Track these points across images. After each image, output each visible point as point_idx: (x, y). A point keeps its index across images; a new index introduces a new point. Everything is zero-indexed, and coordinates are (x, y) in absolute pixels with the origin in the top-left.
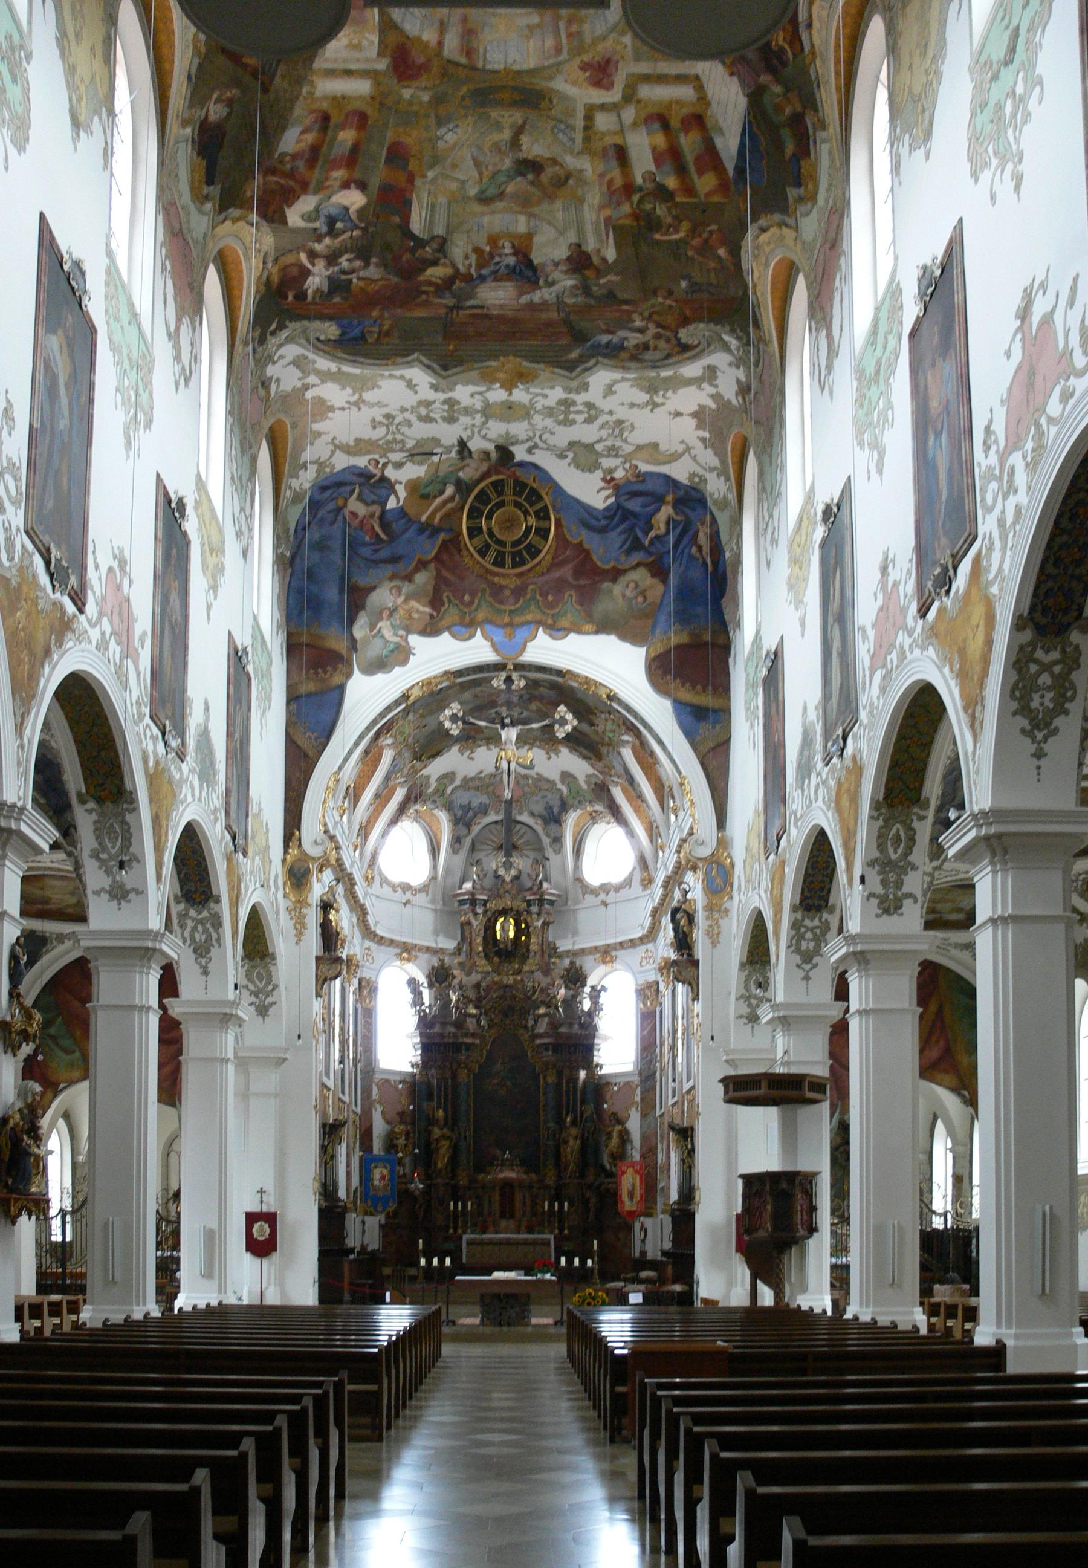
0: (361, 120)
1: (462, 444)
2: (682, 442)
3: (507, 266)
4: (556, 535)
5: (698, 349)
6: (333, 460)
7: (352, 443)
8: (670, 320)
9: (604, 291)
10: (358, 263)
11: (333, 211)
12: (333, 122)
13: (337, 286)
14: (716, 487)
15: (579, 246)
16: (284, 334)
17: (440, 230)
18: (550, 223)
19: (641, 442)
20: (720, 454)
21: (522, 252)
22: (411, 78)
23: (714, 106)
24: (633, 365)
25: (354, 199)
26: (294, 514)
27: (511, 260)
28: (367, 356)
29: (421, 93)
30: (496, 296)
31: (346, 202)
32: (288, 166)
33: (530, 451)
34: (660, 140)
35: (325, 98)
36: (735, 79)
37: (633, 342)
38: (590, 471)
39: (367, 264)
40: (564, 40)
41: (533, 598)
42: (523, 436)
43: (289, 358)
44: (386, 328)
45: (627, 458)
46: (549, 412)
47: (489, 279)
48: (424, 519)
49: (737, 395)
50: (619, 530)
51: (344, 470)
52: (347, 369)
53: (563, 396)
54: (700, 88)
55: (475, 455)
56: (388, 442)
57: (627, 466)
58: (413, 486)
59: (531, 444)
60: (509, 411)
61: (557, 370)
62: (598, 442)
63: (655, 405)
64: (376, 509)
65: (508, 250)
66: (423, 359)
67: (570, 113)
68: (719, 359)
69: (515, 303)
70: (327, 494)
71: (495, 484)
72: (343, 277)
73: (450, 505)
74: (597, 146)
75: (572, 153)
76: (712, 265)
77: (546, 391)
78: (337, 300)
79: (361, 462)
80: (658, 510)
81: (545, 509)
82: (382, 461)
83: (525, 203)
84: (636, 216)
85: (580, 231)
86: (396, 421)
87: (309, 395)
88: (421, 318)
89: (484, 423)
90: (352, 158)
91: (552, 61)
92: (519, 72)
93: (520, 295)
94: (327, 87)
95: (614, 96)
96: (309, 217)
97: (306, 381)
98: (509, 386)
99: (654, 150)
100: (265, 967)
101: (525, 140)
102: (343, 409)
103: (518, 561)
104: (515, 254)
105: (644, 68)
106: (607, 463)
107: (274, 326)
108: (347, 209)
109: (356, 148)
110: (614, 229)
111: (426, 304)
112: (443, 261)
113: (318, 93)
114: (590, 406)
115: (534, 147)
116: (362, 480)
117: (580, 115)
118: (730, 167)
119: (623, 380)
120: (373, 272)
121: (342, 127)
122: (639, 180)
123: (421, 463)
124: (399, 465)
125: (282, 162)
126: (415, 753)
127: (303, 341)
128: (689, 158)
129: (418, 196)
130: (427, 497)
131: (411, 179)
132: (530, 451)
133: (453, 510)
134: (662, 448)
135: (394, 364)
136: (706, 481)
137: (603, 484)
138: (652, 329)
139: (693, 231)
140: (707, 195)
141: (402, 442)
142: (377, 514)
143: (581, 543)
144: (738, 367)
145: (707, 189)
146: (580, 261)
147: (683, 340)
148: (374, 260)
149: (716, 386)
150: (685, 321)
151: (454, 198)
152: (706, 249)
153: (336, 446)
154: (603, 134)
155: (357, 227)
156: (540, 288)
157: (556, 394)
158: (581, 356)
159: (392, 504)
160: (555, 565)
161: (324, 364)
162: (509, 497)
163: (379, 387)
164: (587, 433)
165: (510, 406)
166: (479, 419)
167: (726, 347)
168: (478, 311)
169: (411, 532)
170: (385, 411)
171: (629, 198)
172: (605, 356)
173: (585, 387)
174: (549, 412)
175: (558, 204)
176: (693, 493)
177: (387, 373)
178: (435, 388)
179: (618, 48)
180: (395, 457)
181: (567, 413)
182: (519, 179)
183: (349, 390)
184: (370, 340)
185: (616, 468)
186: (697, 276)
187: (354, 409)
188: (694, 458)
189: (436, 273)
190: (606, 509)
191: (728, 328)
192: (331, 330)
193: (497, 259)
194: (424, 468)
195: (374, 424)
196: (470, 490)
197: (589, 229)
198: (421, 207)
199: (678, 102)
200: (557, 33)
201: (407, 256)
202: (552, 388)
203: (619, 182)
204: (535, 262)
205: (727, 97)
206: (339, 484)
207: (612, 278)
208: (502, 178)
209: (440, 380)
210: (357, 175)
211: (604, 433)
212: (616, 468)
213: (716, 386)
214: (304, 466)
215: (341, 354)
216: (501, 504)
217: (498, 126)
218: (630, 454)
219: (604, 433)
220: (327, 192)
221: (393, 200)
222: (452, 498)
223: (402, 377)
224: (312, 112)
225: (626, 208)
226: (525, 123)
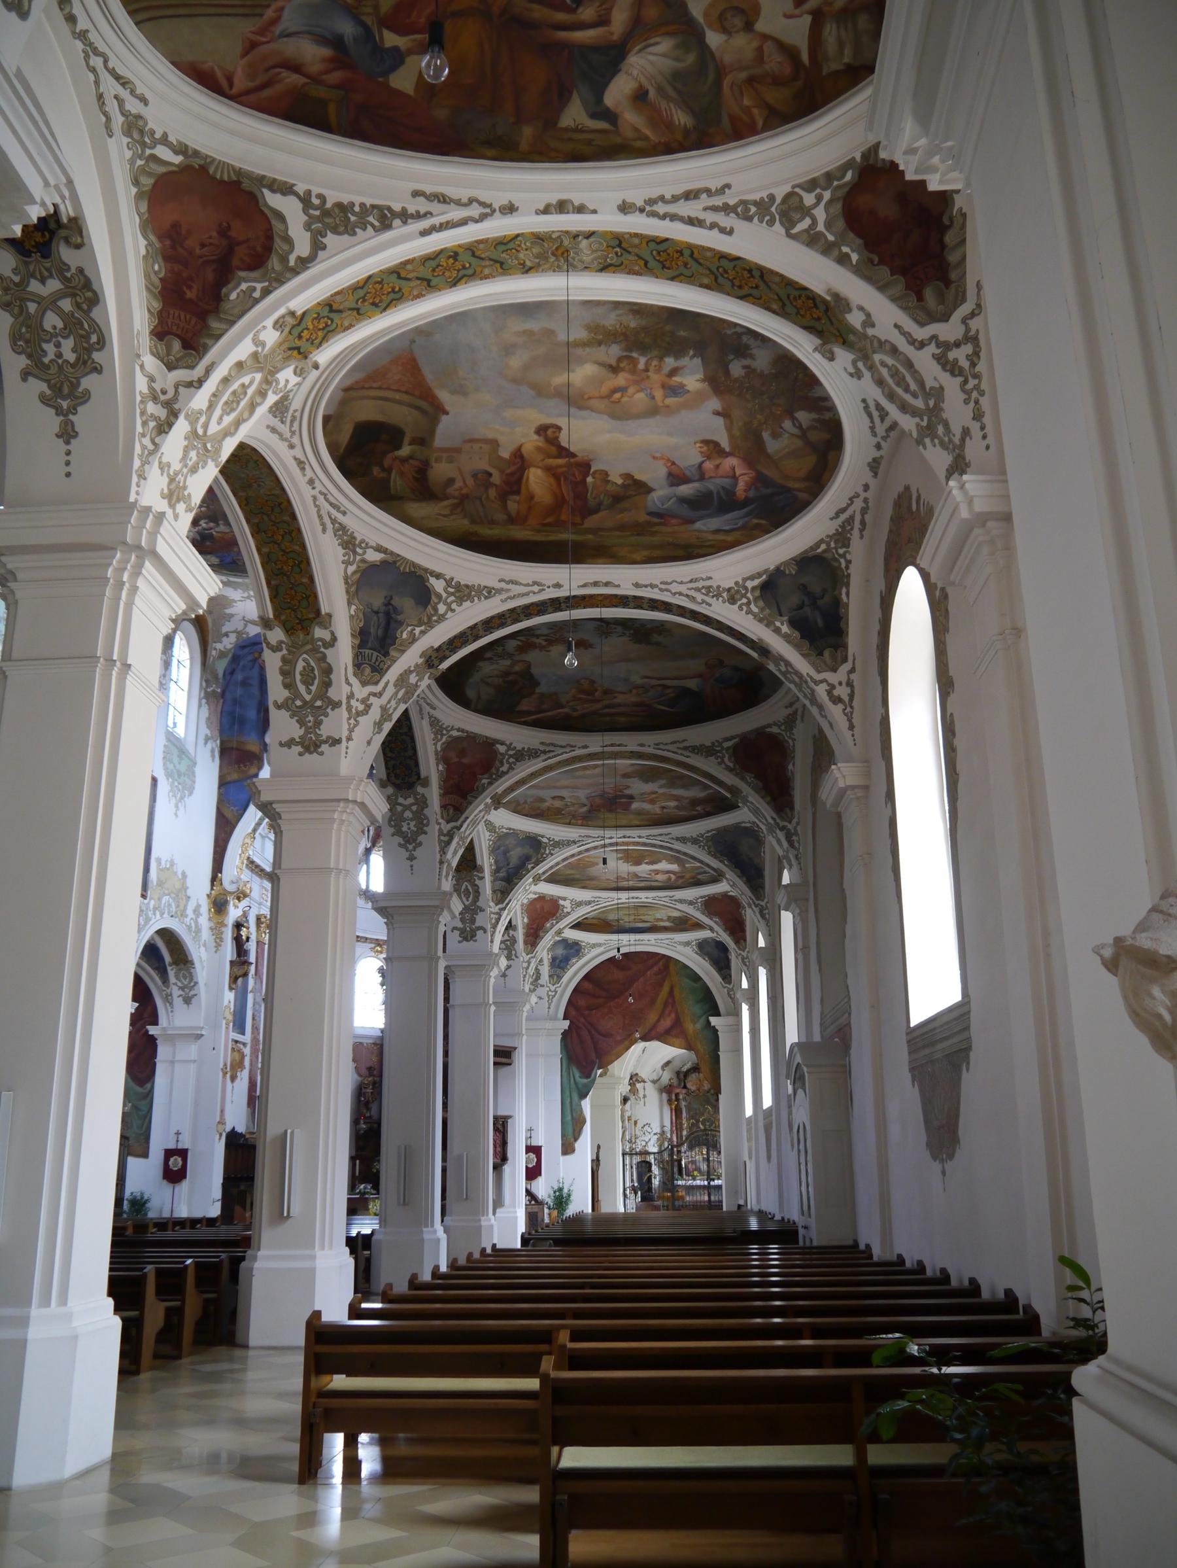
6: (247, 630)
10: (212, 525)
26: (221, 666)
39: (218, 525)
52: (232, 579)
70: (246, 650)
100: (188, 970)
214: (226, 635)
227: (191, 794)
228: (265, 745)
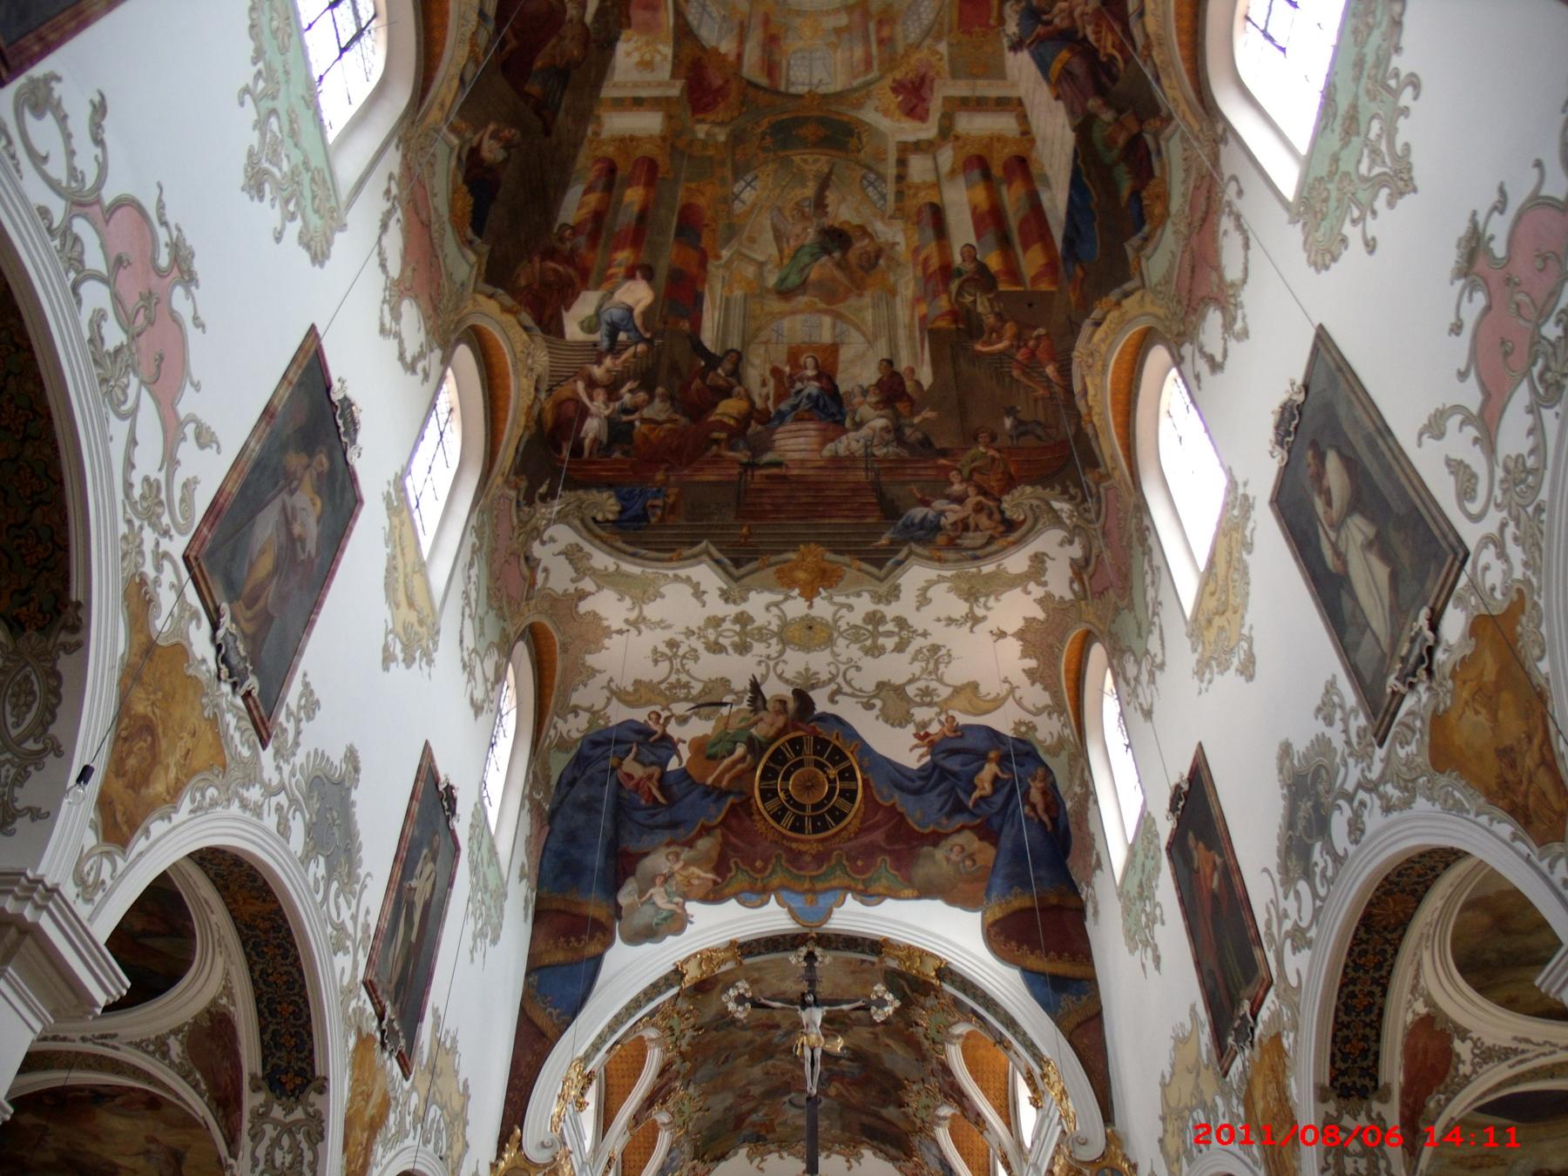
0: (649, 170)
1: (755, 687)
2: (1006, 681)
3: (809, 395)
4: (864, 797)
5: (1024, 528)
6: (609, 711)
7: (630, 689)
8: (993, 483)
9: (919, 435)
10: (642, 395)
11: (617, 314)
12: (620, 173)
13: (618, 431)
14: (1048, 730)
15: (890, 363)
16: (556, 506)
17: (734, 343)
18: (858, 329)
19: (958, 683)
20: (1051, 687)
21: (826, 375)
22: (705, 108)
23: (1039, 143)
24: (951, 555)
25: (638, 295)
27: (813, 388)
28: (646, 545)
29: (717, 130)
30: (796, 445)
31: (629, 301)
32: (568, 245)
33: (832, 700)
34: (980, 195)
35: (613, 140)
36: (1061, 104)
37: (952, 518)
38: (901, 725)
40: (874, 49)
41: (839, 863)
42: (824, 676)
43: (560, 546)
44: (670, 500)
45: (943, 707)
46: (855, 634)
47: (789, 418)
48: (709, 781)
49: (1072, 582)
50: (938, 790)
51: (619, 725)
53: (871, 607)
54: (1023, 118)
55: (770, 706)
56: (672, 687)
57: (943, 718)
58: (699, 746)
59: (833, 686)
60: (811, 634)
61: (865, 566)
62: (910, 682)
63: (976, 620)
64: (656, 771)
65: (810, 373)
66: (713, 549)
67: (880, 156)
68: (1048, 541)
69: (815, 456)
70: (599, 751)
71: (792, 742)
72: (625, 418)
73: (740, 766)
74: (912, 204)
75: (882, 218)
76: (1041, 392)
77: (852, 600)
78: (617, 455)
79: (640, 715)
80: (981, 768)
81: (851, 769)
82: (664, 714)
83: (830, 295)
84: (954, 315)
85: (893, 343)
86: (681, 652)
87: (584, 607)
88: (709, 483)
89: (782, 653)
90: (638, 234)
91: (860, 80)
92: (825, 96)
93: (823, 444)
94: (618, 123)
95: (928, 131)
96: (589, 326)
97: (581, 585)
98: (809, 595)
99: (974, 210)
101: (831, 197)
102: (620, 632)
103: (820, 825)
104: (817, 378)
105: (961, 89)
106: (921, 714)
107: (543, 489)
108: (630, 310)
109: (643, 215)
110: (931, 331)
111: (717, 460)
112: (738, 389)
113: (605, 135)
114: (901, 622)
115: (843, 212)
116: (641, 738)
117: (892, 157)
118: (1058, 234)
119: (941, 579)
120: (658, 409)
121: (629, 182)
122: (958, 259)
123: (708, 718)
124: (683, 720)
125: (561, 239)
126: (696, 1147)
127: (577, 522)
128: (1013, 222)
129: (711, 288)
130: (713, 758)
131: (703, 264)
132: (832, 700)
133: (743, 772)
134: (983, 690)
135: (680, 559)
136: (1034, 728)
137: (916, 741)
138: (974, 499)
139: (1018, 337)
140: (1035, 279)
141: (687, 686)
142: (657, 775)
143: (893, 806)
144: (1071, 542)
145: (1033, 273)
146: (892, 389)
147: (1008, 514)
148: (660, 390)
149: (1045, 584)
150: (1010, 483)
151: (752, 308)
152: (1032, 366)
153: (613, 693)
154: (918, 188)
155: (642, 339)
156: (845, 431)
157: (864, 604)
158: (892, 543)
159: (673, 765)
160: (860, 831)
161: (601, 560)
162: (808, 755)
163: (662, 596)
164: (896, 667)
165: (810, 624)
166: (775, 647)
167: (1057, 521)
168: (774, 471)
169: (695, 795)
170: (668, 635)
171: (946, 290)
172: (919, 541)
173: (894, 593)
174: (855, 634)
175: (867, 299)
176: (1020, 746)
177: (671, 573)
178: (726, 596)
179: (934, 59)
180: (680, 708)
181: (875, 635)
182: (824, 259)
183: (628, 602)
184: (653, 520)
185: (931, 721)
186: (1025, 415)
187: (634, 632)
188: (1019, 703)
189: (729, 408)
190: (922, 769)
191: (1058, 489)
192: (607, 504)
193: (798, 386)
194: (712, 723)
195: (657, 657)
196: (763, 750)
197: (902, 333)
198: (713, 302)
199: (999, 139)
200: (866, 39)
201: (697, 384)
202: (859, 595)
203: (935, 263)
204: (842, 389)
205: (1054, 135)
206: (618, 742)
207: (928, 414)
208: (806, 259)
209: (734, 585)
210: (645, 258)
211: (917, 668)
212: (931, 721)
213: (1045, 584)
214: (575, 710)
215: (620, 544)
216: (800, 764)
217: (800, 178)
218: (946, 700)
219: (917, 668)
220: (607, 285)
221: (681, 295)
222: (742, 759)
223: (688, 580)
224: (597, 160)
225: (944, 303)
226: (830, 173)
227: (494, 941)
228: (618, 908)
